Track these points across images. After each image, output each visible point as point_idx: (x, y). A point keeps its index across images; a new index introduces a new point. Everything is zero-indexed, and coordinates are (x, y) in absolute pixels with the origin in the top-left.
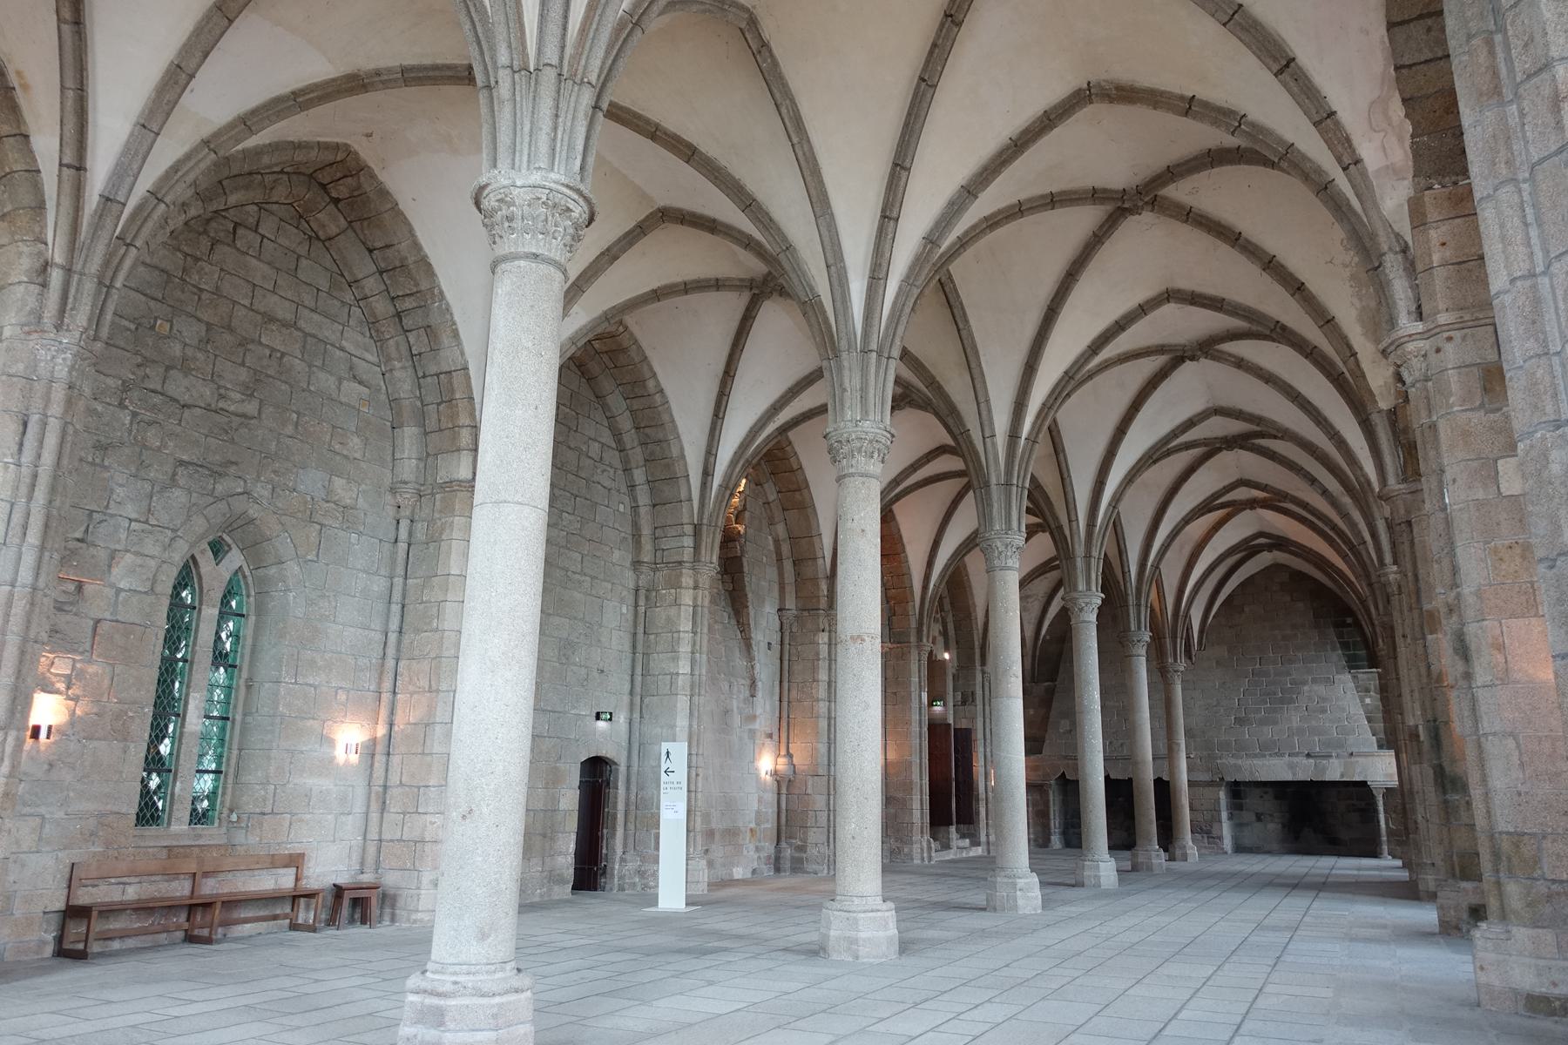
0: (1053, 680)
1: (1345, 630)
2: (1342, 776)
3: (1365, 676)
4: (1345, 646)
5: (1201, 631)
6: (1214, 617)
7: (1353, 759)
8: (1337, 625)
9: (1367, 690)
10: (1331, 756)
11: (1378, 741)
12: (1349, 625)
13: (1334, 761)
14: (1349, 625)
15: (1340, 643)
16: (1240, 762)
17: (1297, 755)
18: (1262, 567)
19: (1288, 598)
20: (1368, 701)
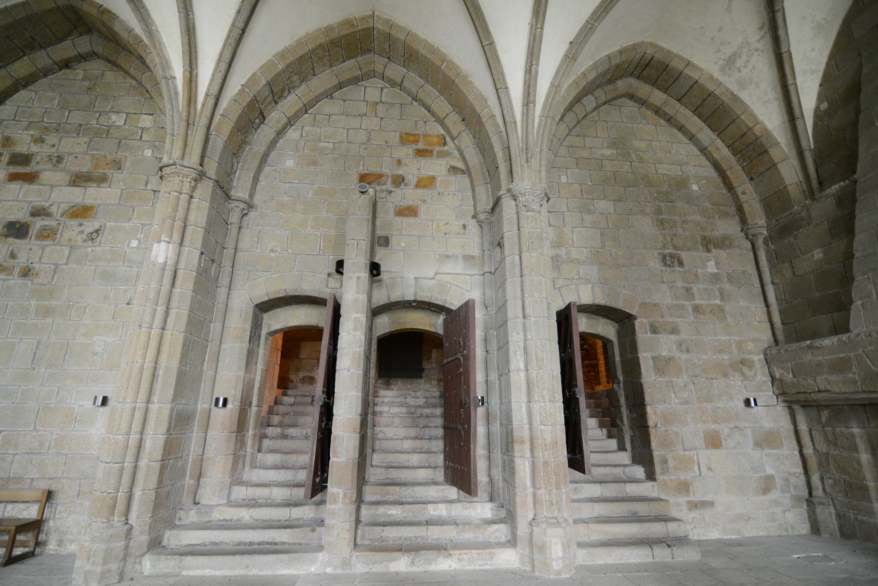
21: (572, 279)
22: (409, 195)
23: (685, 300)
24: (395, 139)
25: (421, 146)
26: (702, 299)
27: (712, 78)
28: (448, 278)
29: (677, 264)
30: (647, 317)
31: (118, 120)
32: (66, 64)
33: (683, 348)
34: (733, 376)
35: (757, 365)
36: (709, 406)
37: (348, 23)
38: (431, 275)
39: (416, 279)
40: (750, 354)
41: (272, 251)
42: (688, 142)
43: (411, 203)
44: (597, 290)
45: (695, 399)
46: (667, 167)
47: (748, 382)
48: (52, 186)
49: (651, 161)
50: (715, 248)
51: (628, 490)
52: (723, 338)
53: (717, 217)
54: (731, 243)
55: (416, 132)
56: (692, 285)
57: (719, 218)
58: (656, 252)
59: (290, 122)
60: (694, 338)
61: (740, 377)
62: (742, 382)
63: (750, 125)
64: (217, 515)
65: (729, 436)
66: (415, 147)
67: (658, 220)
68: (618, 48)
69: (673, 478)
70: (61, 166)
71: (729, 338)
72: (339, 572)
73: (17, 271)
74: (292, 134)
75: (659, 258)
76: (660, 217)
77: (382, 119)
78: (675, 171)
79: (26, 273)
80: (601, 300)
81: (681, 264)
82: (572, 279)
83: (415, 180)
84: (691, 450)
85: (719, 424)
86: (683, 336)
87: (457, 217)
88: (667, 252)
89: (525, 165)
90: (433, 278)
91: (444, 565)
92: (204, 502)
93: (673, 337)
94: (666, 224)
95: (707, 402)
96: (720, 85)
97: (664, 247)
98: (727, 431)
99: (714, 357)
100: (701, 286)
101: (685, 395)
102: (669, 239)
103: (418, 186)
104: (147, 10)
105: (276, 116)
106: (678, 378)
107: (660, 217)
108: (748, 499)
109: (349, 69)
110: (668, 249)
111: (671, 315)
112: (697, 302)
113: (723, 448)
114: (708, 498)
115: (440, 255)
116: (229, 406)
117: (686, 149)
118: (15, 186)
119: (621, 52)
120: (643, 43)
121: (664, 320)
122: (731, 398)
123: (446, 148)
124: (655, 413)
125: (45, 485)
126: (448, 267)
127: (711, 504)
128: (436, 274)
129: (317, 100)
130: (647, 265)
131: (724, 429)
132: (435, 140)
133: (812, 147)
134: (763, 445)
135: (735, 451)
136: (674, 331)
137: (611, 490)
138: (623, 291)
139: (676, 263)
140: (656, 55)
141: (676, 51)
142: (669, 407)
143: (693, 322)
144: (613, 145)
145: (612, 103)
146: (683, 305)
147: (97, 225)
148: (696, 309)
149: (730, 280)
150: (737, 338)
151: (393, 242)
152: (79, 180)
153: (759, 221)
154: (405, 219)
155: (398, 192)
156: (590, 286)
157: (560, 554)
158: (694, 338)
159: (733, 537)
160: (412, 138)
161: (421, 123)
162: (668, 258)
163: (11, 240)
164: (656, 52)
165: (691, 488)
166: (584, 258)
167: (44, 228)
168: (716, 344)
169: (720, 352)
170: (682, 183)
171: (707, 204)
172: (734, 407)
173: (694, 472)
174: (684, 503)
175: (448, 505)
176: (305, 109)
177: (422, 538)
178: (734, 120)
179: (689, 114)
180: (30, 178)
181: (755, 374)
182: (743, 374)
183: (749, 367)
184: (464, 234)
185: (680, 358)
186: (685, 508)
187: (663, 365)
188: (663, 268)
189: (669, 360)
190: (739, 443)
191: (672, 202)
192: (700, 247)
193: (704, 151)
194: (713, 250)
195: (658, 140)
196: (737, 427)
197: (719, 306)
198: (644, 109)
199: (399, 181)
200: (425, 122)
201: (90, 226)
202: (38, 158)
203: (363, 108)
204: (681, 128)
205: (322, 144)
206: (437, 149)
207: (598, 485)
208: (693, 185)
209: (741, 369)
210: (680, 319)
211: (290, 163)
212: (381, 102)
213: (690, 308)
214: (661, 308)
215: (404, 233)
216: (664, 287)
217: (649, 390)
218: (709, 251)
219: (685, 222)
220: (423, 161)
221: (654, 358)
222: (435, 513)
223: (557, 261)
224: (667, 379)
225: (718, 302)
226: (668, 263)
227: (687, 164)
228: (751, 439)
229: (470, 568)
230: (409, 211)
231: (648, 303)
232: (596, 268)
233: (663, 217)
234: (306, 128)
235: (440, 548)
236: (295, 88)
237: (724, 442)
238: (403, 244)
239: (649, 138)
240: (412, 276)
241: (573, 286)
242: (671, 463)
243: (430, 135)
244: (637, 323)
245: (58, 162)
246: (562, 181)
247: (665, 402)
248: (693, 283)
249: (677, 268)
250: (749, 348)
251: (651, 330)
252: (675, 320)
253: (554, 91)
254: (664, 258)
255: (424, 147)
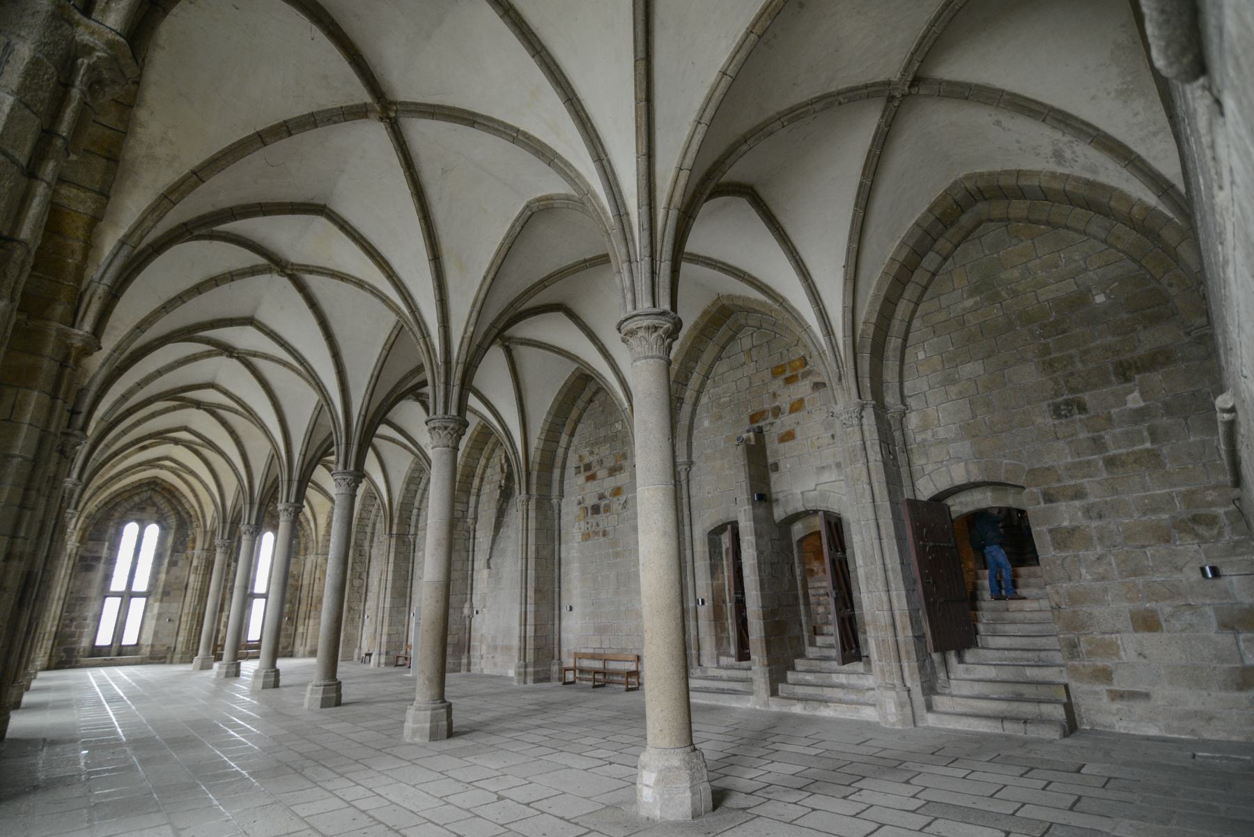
21: (942, 461)
22: (786, 421)
23: (1092, 455)
24: (767, 374)
25: (788, 374)
26: (1120, 448)
27: (1053, 175)
28: (826, 487)
29: (1077, 412)
30: (1037, 486)
31: (618, 426)
32: (591, 401)
33: (1094, 514)
34: (1180, 539)
35: (1224, 520)
36: (1140, 581)
37: (705, 313)
38: (813, 487)
39: (802, 493)
40: (1210, 507)
41: (709, 493)
43: (788, 428)
44: (972, 467)
45: (1116, 573)
46: (1053, 287)
47: (1211, 545)
48: (603, 479)
49: (1028, 290)
50: (1139, 372)
51: (1028, 673)
52: (1158, 492)
53: (1140, 327)
54: (1167, 358)
55: (783, 363)
56: (1102, 433)
57: (1145, 327)
58: (1044, 405)
59: (699, 393)
60: (1108, 499)
61: (1193, 539)
62: (1200, 546)
64: (710, 673)
65: (1172, 616)
66: (783, 377)
67: (1044, 363)
68: (926, 207)
69: (1086, 663)
70: (603, 465)
71: (1167, 490)
72: (763, 709)
73: (601, 533)
74: (704, 400)
75: (1050, 411)
76: (1047, 358)
77: (756, 362)
78: (1069, 287)
79: (605, 534)
80: (976, 476)
81: (1082, 408)
82: (942, 461)
83: (789, 406)
84: (1113, 633)
85: (1157, 601)
86: (1092, 499)
87: (826, 429)
88: (1060, 399)
90: (815, 490)
91: (827, 712)
92: (704, 665)
93: (1077, 503)
94: (1056, 365)
95: (1136, 575)
96: (1067, 180)
97: (1056, 395)
98: (1168, 610)
99: (1144, 519)
100: (1118, 430)
101: (1101, 570)
102: (1062, 382)
103: (791, 411)
104: (604, 378)
105: (689, 394)
106: (1087, 550)
107: (1047, 358)
108: (1209, 695)
109: (722, 333)
110: (1063, 395)
111: (1072, 477)
112: (1112, 452)
113: (1162, 631)
114: (1141, 688)
115: (817, 468)
116: (706, 604)
118: (589, 484)
119: (930, 210)
120: (955, 183)
121: (1062, 484)
122: (1176, 568)
123: (808, 367)
124: (1057, 592)
125: (635, 652)
126: (826, 477)
127: (1147, 696)
128: (817, 485)
129: (711, 366)
130: (1033, 424)
131: (1165, 608)
132: (798, 363)
134: (1237, 627)
135: (1184, 635)
136: (1079, 494)
137: (1007, 674)
138: (1005, 461)
139: (1075, 410)
140: (979, 184)
141: (998, 168)
142: (1077, 584)
143: (1106, 479)
144: (974, 291)
145: (970, 238)
146: (1089, 462)
147: (625, 497)
148: (1111, 463)
149: (1169, 410)
150: (1183, 489)
151: (781, 465)
152: (613, 471)
154: (787, 444)
155: (778, 421)
156: (962, 464)
157: (894, 711)
158: (1108, 499)
159: (1183, 737)
160: (780, 370)
161: (785, 352)
162: (1062, 407)
163: (595, 516)
164: (976, 182)
165: (1113, 676)
166: (953, 436)
167: (606, 506)
168: (1147, 501)
169: (1154, 510)
170: (1080, 300)
171: (1125, 316)
172: (1183, 579)
173: (1120, 658)
174: (1104, 691)
175: (847, 676)
176: (706, 377)
177: (821, 696)
180: (592, 478)
181: (1220, 534)
182: (1197, 535)
183: (1207, 525)
184: (834, 443)
185: (1088, 527)
186: (1105, 699)
188: (1056, 422)
189: (1072, 531)
190: (1191, 625)
192: (1113, 378)
194: (1137, 377)
195: (1037, 257)
196: (1190, 605)
197: (1147, 450)
199: (777, 412)
200: (788, 350)
201: (622, 498)
202: (593, 464)
203: (742, 358)
205: (722, 400)
206: (801, 371)
207: (992, 667)
208: (1096, 297)
209: (1193, 529)
210: (1086, 480)
211: (706, 423)
212: (753, 347)
213: (1101, 463)
214: (1056, 471)
215: (787, 456)
216: (1061, 444)
217: (1048, 568)
218: (1127, 379)
219: (1086, 352)
220: (791, 387)
221: (1050, 531)
222: (838, 681)
223: (924, 446)
224: (1071, 553)
225: (1148, 445)
226: (1063, 413)
227: (1086, 270)
228: (1214, 620)
229: (842, 717)
230: (788, 436)
231: (1039, 468)
232: (967, 443)
233: (1052, 356)
234: (711, 391)
235: (825, 701)
236: (694, 368)
237: (1164, 624)
238: (788, 466)
239: (1025, 260)
240: (799, 492)
241: (944, 469)
242: (1083, 647)
243: (793, 361)
245: (602, 463)
246: (920, 358)
247: (1070, 580)
248: (1105, 430)
249: (1078, 417)
250: (1210, 499)
251: (1045, 500)
252: (1079, 481)
254: (1057, 411)
255: (790, 374)
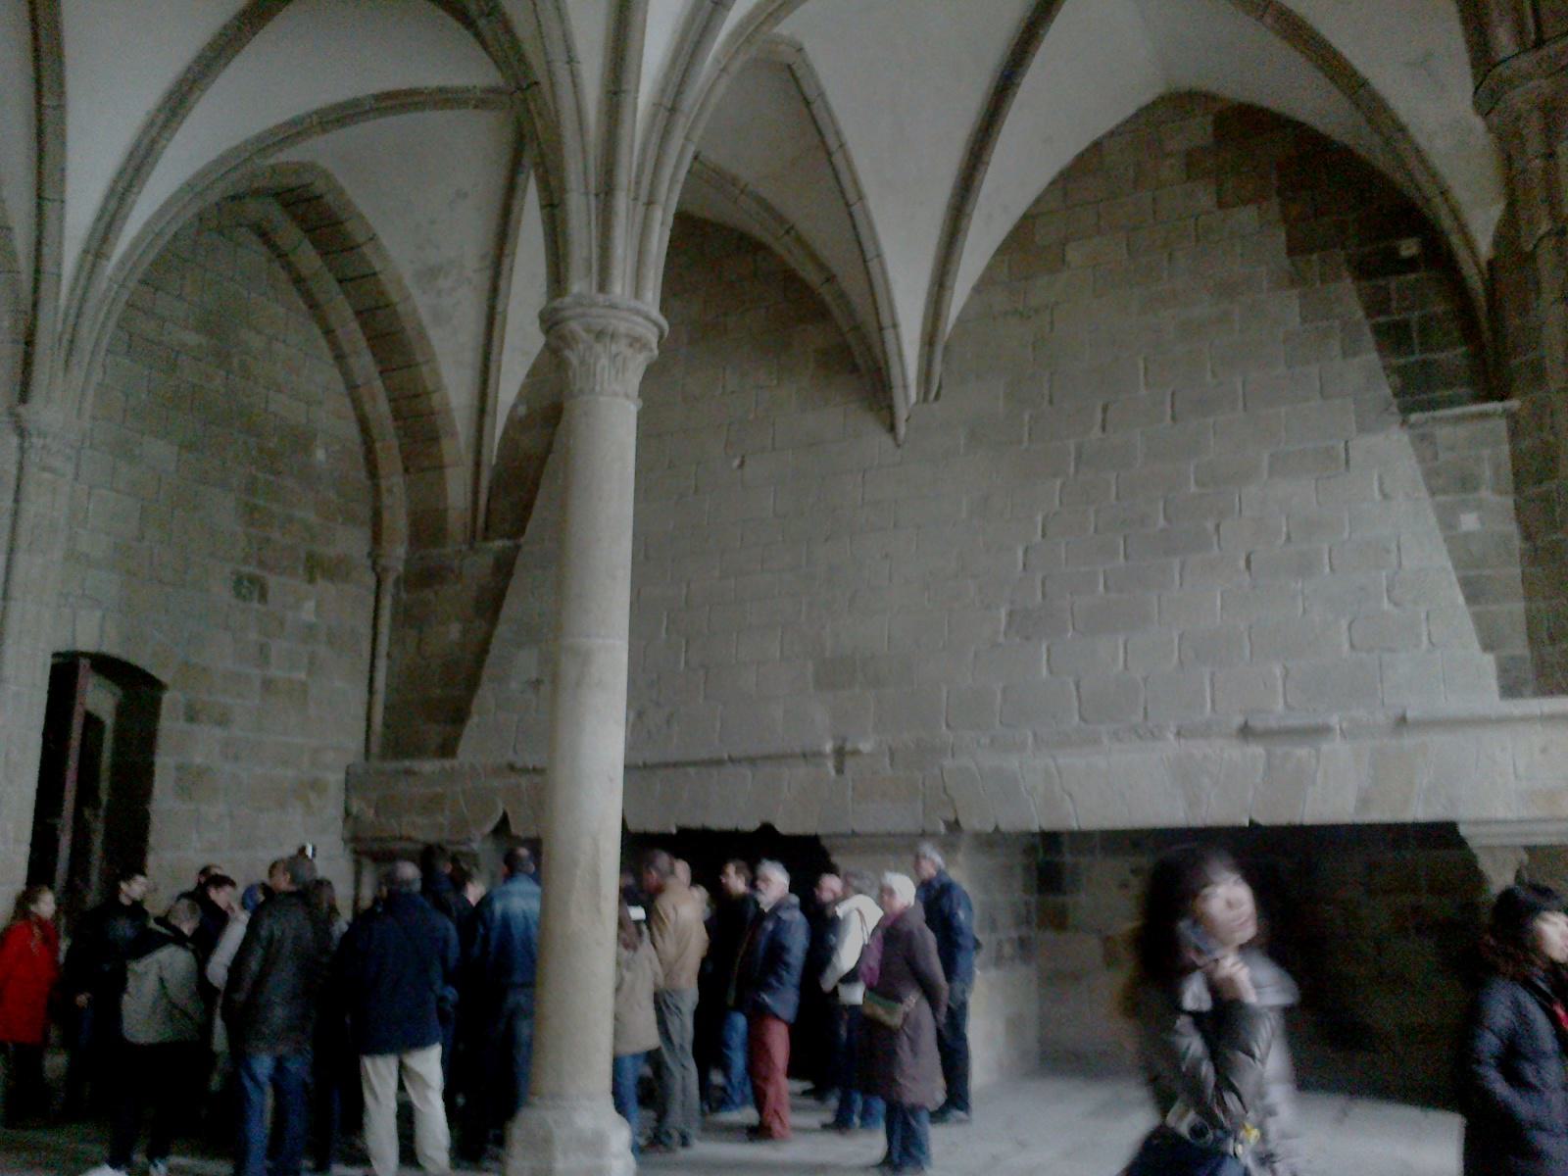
0: (518, 529)
1: (1393, 283)
2: (1364, 802)
3: (1462, 432)
4: (1393, 337)
5: (929, 340)
6: (978, 289)
7: (1409, 741)
8: (1363, 270)
9: (1466, 483)
10: (1321, 731)
11: (1503, 670)
12: (1411, 264)
13: (1336, 749)
14: (1411, 264)
15: (1377, 330)
16: (1013, 762)
17: (1205, 731)
18: (1131, 111)
19: (1205, 198)
20: (1469, 522)
42: (332, 362)
53: (340, 520)
63: (431, 387)
67: (247, 505)
81: (263, 597)
88: (246, 569)
89: (61, 374)
93: (218, 732)
97: (245, 561)
117: (324, 375)
133: (494, 462)
136: (223, 720)
139: (256, 595)
148: (268, 685)
153: (397, 553)
156: (98, 614)
170: (302, 440)
178: (410, 365)
179: (349, 313)
187: (191, 780)
191: (278, 473)
193: (352, 388)
198: (276, 266)
204: (328, 332)
218: (311, 580)
225: (302, 675)
244: (167, 698)
249: (255, 605)
253: (147, 241)
254: (239, 582)
